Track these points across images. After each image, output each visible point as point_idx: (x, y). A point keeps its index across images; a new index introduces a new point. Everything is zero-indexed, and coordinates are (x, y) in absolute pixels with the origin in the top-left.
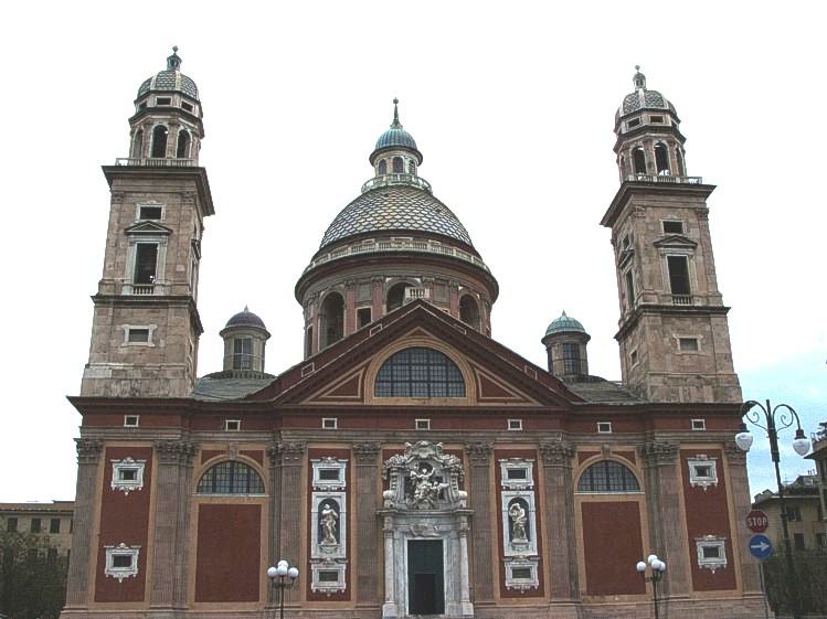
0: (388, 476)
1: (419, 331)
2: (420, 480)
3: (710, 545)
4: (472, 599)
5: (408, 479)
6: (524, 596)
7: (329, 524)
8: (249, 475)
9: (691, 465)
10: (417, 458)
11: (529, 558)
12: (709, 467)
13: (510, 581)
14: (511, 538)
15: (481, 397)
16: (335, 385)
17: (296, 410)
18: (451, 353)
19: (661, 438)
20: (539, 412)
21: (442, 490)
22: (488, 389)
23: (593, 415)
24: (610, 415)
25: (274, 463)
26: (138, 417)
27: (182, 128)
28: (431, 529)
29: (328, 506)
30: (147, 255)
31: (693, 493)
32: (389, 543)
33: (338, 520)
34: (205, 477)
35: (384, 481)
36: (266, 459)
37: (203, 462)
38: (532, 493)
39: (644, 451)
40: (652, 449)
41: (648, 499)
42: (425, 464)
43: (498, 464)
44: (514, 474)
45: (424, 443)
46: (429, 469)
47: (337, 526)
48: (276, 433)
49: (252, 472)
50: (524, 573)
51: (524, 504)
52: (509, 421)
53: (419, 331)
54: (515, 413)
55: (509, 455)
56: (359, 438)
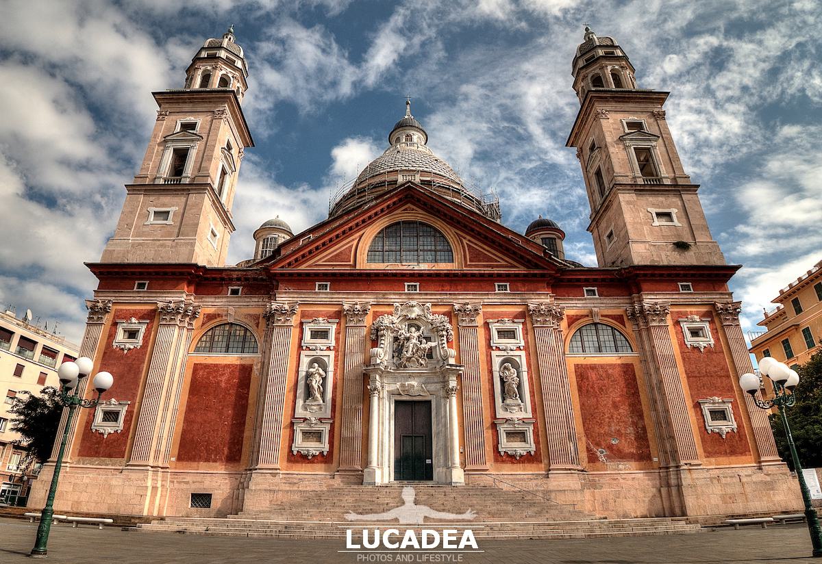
0: (377, 336)
1: (409, 207)
2: (408, 339)
3: (716, 407)
4: (463, 465)
5: (396, 339)
6: (519, 462)
7: (316, 383)
8: (245, 335)
9: (685, 326)
10: (406, 318)
11: (523, 421)
12: (701, 329)
13: (506, 445)
14: (504, 399)
15: (468, 263)
16: (330, 254)
17: (291, 275)
18: (439, 224)
19: (649, 300)
20: (525, 275)
21: (431, 349)
22: (476, 256)
23: (578, 280)
24: (595, 280)
25: (268, 325)
26: (147, 282)
27: (224, 72)
28: (415, 386)
29: (316, 365)
30: (181, 156)
31: (690, 354)
32: (375, 400)
33: (324, 379)
34: (204, 339)
35: (373, 341)
36: (262, 322)
37: (203, 324)
38: (523, 353)
39: (633, 314)
40: (642, 310)
41: (644, 361)
42: (413, 324)
43: (487, 325)
44: (503, 334)
45: (414, 303)
46: (418, 329)
47: (324, 385)
48: (272, 297)
49: (248, 334)
50: (520, 435)
51: (517, 366)
52: (496, 284)
53: (409, 207)
54: (500, 277)
55: (499, 318)
56: (349, 300)
